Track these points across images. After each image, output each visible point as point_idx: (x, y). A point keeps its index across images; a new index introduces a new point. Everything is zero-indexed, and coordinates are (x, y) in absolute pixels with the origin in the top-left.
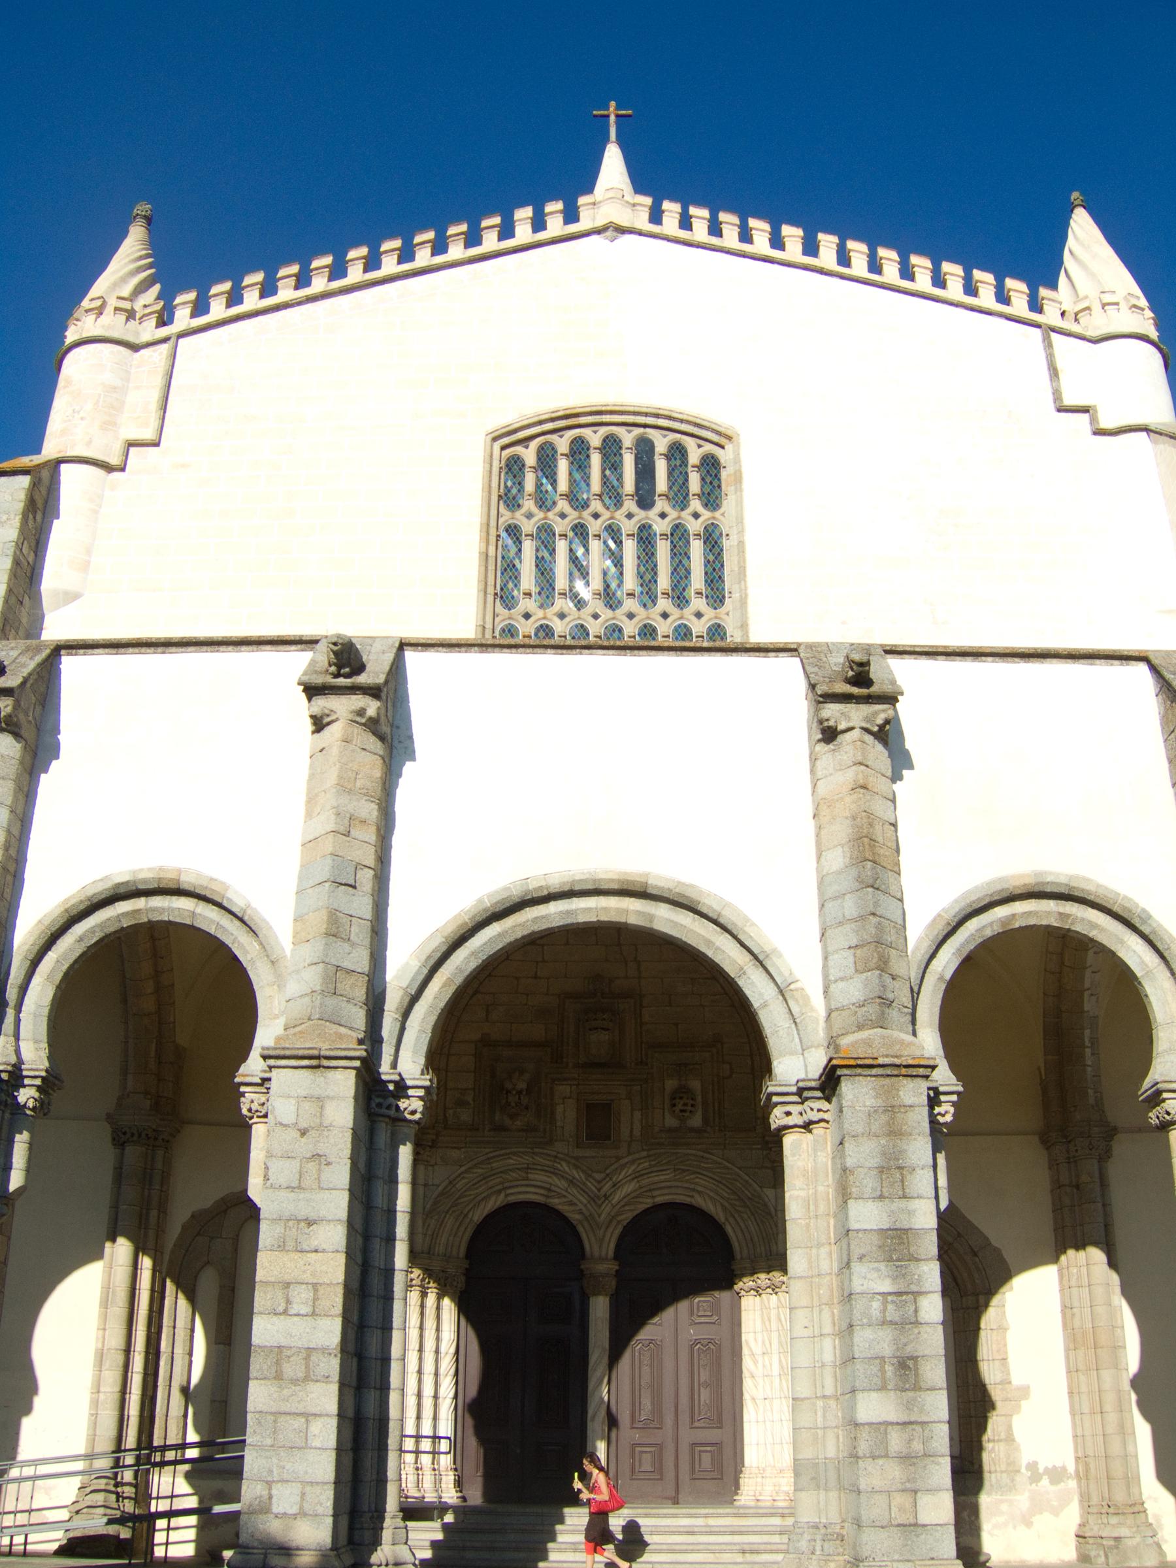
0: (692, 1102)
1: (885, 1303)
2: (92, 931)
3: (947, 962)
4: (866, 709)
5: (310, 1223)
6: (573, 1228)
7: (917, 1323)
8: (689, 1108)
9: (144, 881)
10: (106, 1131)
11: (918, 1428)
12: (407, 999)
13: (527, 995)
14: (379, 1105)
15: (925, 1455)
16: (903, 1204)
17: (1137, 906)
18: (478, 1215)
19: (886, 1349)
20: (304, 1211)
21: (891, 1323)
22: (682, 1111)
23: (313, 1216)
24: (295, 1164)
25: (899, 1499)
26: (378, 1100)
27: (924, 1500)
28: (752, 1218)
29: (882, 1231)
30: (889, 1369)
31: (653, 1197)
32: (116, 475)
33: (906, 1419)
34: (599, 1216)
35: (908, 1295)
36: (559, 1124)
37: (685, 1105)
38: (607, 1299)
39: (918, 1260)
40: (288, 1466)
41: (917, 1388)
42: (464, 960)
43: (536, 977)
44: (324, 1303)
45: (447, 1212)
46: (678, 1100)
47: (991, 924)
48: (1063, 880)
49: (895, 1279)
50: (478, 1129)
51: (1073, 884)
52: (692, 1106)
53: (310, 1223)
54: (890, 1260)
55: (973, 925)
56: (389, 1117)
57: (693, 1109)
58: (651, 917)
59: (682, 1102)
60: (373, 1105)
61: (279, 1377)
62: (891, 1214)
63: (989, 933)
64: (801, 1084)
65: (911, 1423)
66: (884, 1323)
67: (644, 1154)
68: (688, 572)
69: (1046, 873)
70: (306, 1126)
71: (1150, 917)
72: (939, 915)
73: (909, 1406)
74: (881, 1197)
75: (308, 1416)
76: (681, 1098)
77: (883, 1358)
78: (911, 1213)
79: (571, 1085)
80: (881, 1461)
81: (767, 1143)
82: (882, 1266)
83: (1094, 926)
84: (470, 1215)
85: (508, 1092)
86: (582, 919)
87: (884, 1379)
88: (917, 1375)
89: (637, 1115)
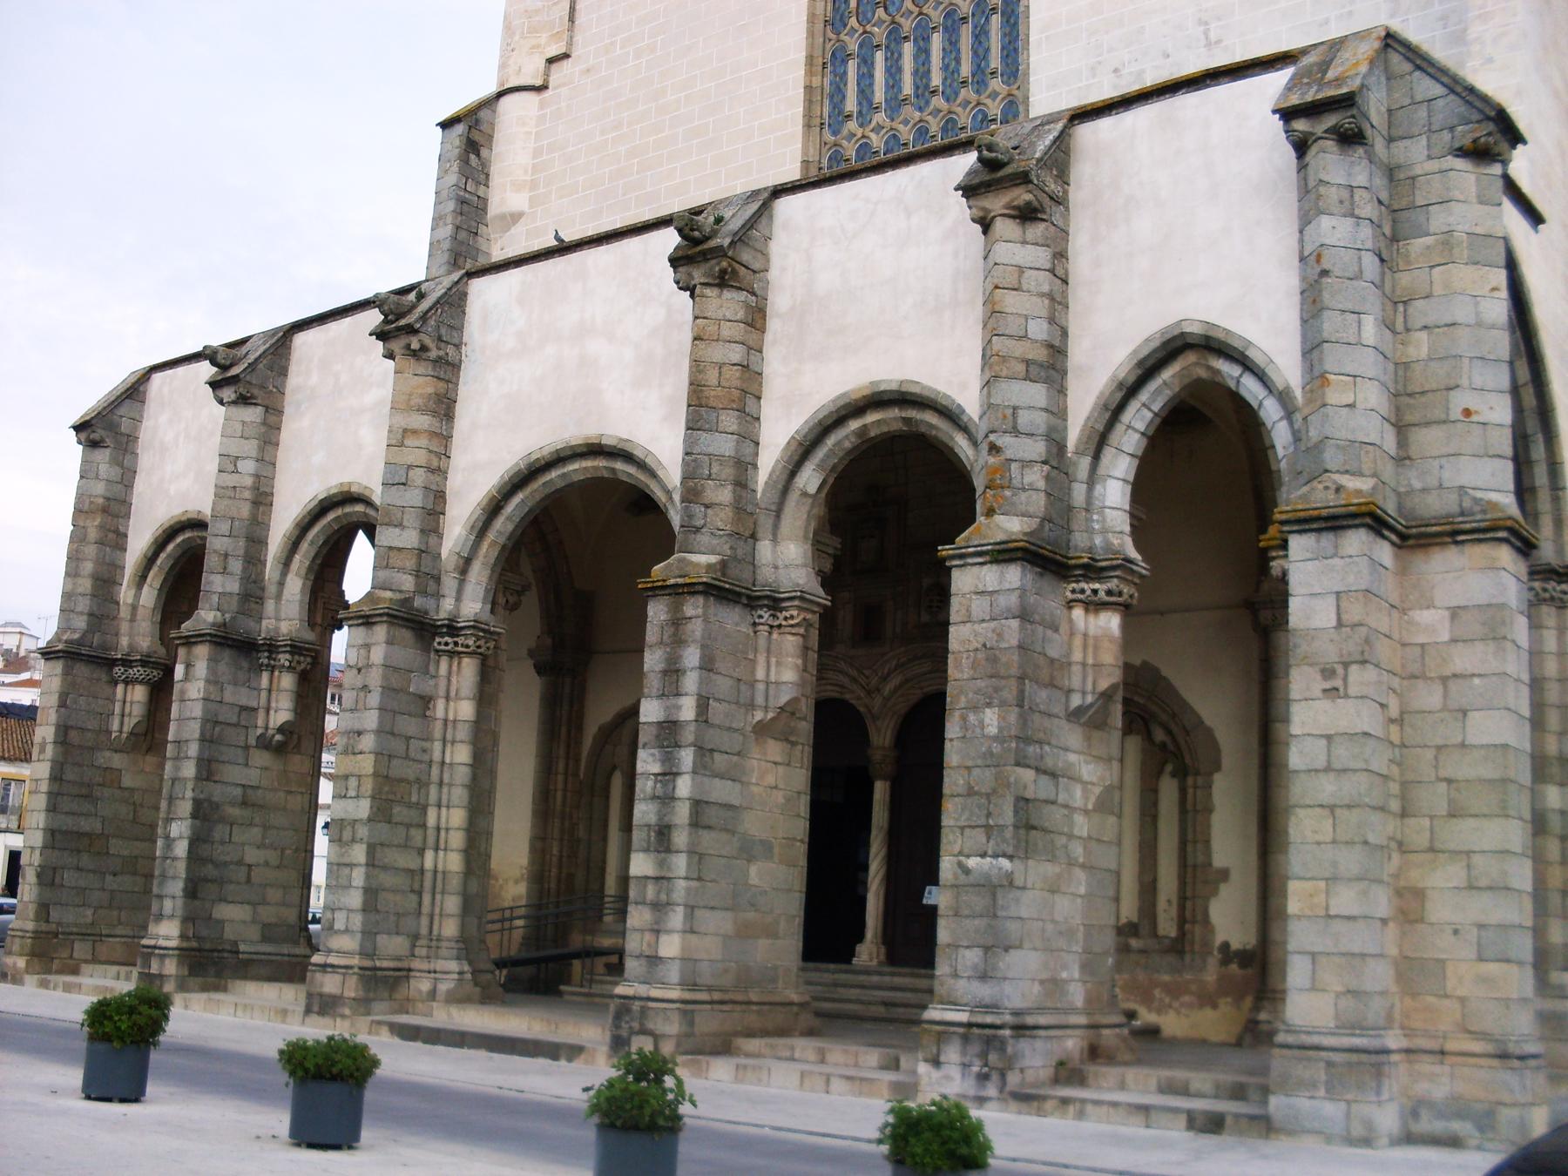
1: (655, 783)
2: (317, 535)
3: (810, 479)
4: (705, 267)
5: (359, 733)
7: (673, 799)
9: (334, 495)
10: (530, 663)
11: (665, 882)
12: (461, 562)
14: (439, 643)
15: (668, 904)
16: (673, 700)
17: (953, 400)
19: (652, 819)
20: (357, 726)
21: (658, 798)
23: (361, 728)
24: (355, 693)
25: (648, 937)
26: (438, 640)
27: (664, 938)
29: (659, 723)
30: (653, 834)
31: (921, 688)
32: (546, 94)
33: (658, 875)
35: (669, 775)
38: (888, 784)
39: (680, 747)
40: (342, 900)
41: (668, 850)
42: (503, 525)
44: (363, 789)
47: (847, 437)
48: (894, 387)
49: (663, 762)
51: (904, 389)
53: (359, 733)
54: (663, 747)
55: (830, 441)
58: (613, 470)
61: (340, 840)
62: (667, 708)
63: (847, 445)
65: (663, 878)
66: (654, 797)
67: (903, 649)
68: (988, 50)
69: (880, 382)
70: (360, 665)
71: (964, 411)
72: (793, 437)
73: (661, 864)
74: (663, 695)
75: (351, 866)
77: (649, 826)
78: (679, 708)
80: (640, 907)
82: (655, 751)
83: (932, 426)
86: (576, 478)
87: (649, 842)
88: (669, 840)
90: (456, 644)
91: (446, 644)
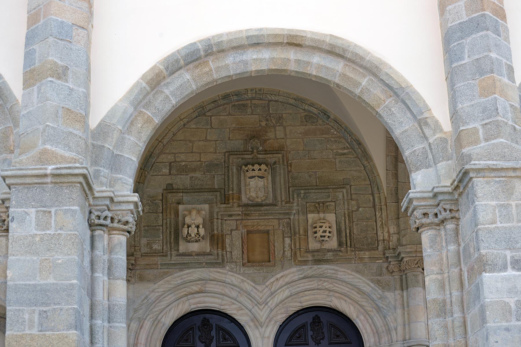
0: (330, 230)
6: (241, 327)
8: (328, 234)
13: (200, 153)
14: (99, 217)
18: (168, 320)
22: (321, 236)
28: (377, 315)
34: (262, 319)
36: (228, 249)
37: (325, 232)
43: (206, 140)
45: (145, 319)
46: (318, 229)
50: (166, 256)
52: (330, 232)
56: (106, 226)
57: (329, 235)
59: (322, 230)
60: (93, 217)
64: (436, 190)
67: (294, 269)
76: (321, 227)
79: (237, 220)
81: (387, 257)
84: (163, 319)
85: (189, 226)
89: (287, 241)
90: (112, 219)
91: (105, 218)
